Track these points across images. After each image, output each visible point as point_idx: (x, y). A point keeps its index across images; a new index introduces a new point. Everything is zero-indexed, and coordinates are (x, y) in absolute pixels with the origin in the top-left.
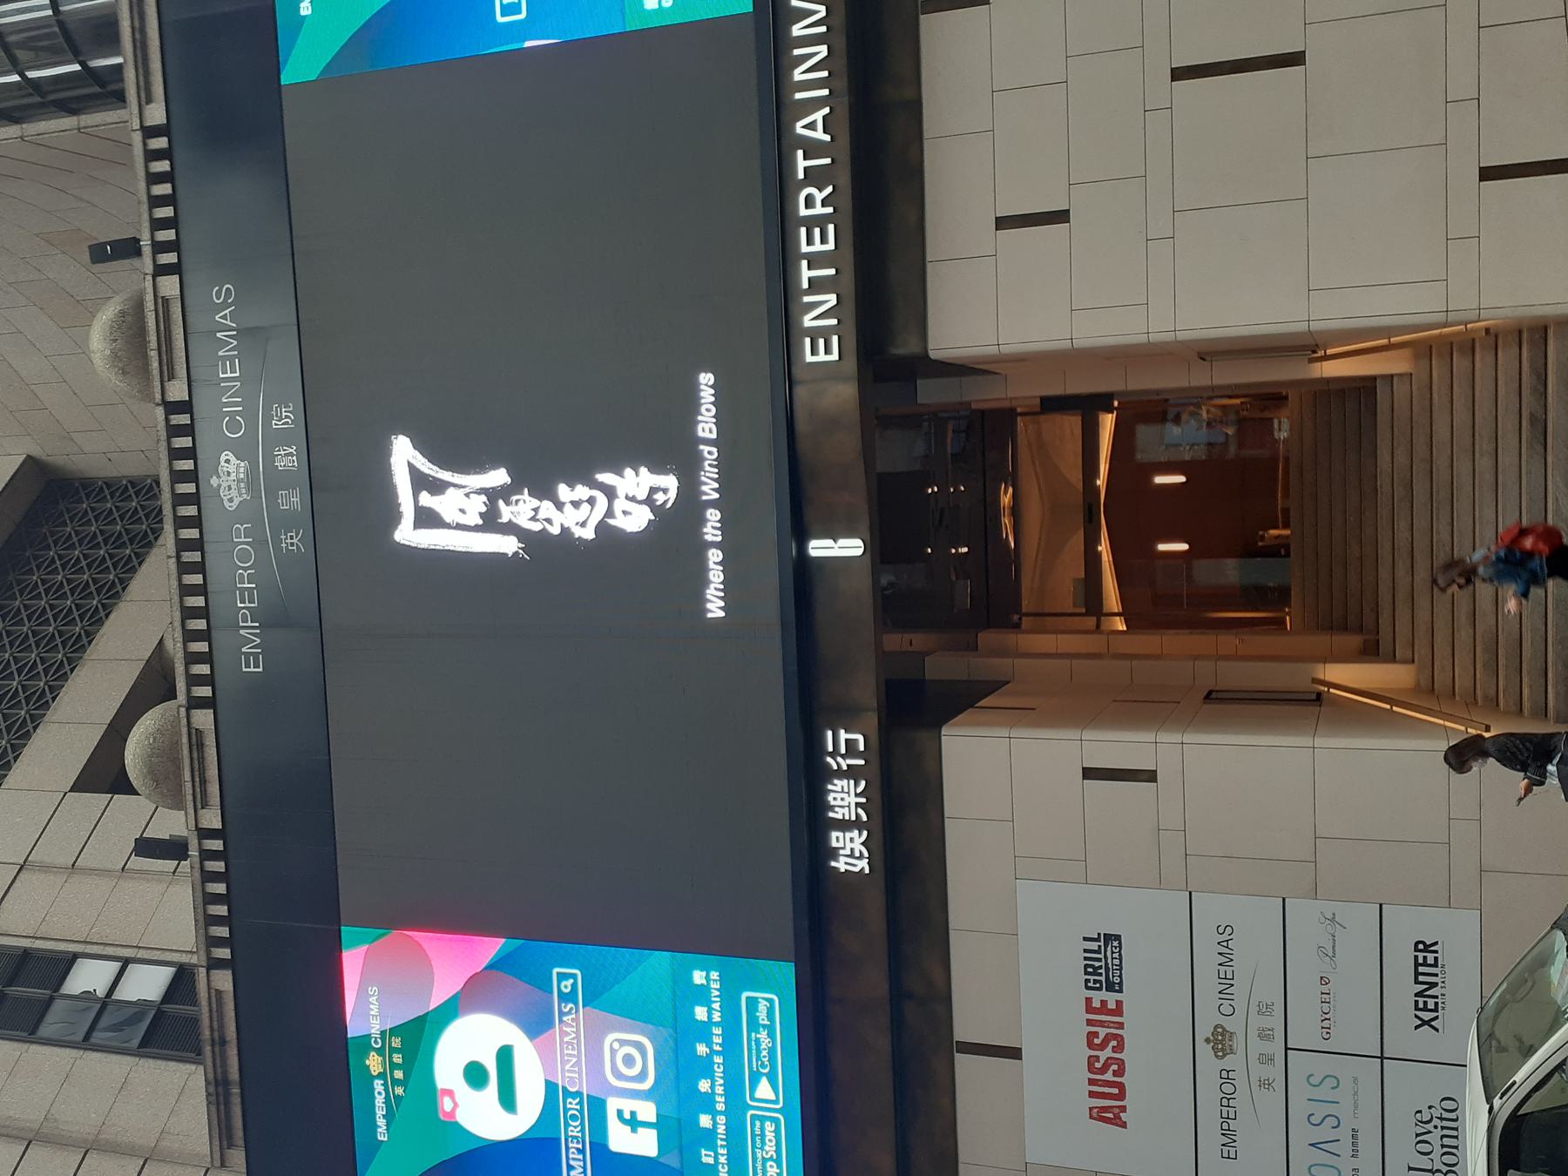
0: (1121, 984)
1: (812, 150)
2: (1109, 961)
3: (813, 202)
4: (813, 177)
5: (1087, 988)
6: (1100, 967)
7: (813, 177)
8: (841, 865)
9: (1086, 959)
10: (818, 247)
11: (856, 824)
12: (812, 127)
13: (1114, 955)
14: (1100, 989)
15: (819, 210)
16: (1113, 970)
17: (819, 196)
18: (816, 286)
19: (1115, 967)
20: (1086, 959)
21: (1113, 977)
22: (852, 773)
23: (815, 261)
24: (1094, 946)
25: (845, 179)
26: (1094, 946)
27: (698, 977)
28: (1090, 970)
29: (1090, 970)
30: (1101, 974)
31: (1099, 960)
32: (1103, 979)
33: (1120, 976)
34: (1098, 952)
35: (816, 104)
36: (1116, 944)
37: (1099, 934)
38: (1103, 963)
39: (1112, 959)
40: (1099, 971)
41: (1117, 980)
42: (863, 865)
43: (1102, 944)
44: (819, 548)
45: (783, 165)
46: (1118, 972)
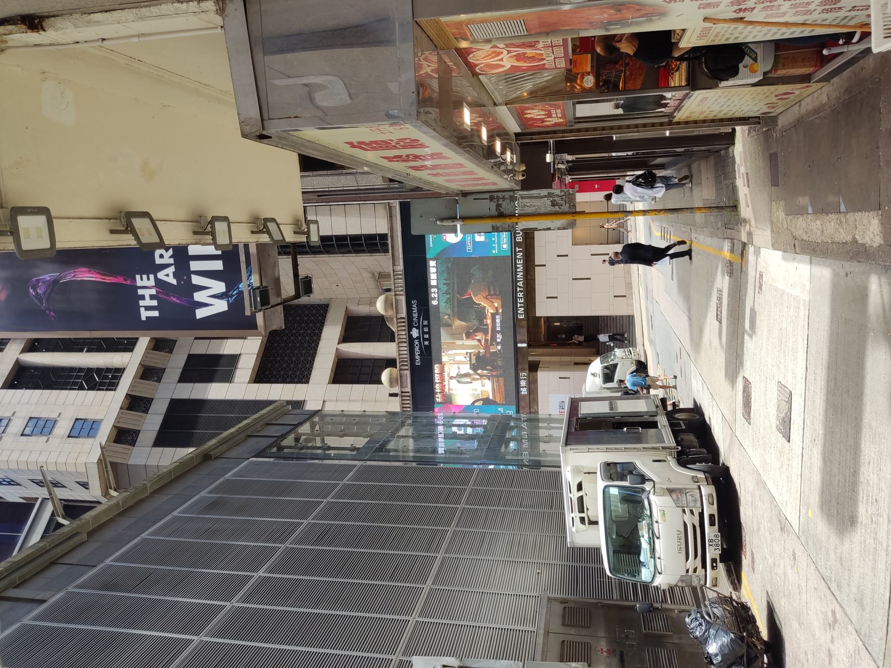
1: (520, 287)
3: (520, 295)
4: (520, 291)
7: (520, 291)
8: (522, 393)
10: (521, 301)
11: (525, 387)
12: (520, 284)
15: (521, 296)
17: (521, 294)
18: (520, 307)
22: (524, 379)
23: (520, 303)
25: (525, 292)
27: (499, 409)
35: (521, 281)
42: (526, 393)
44: (519, 345)
45: (516, 289)
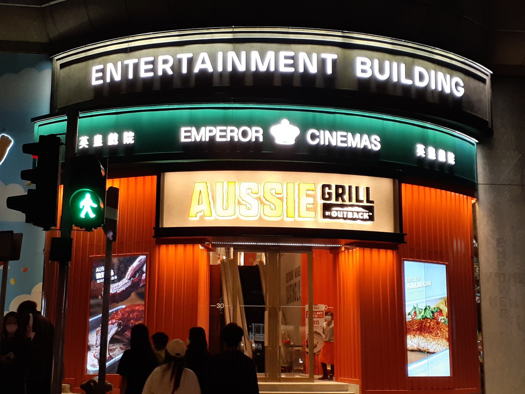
0: (330, 217)
2: (349, 209)
5: (324, 186)
6: (343, 200)
9: (350, 187)
13: (355, 214)
14: (323, 198)
16: (343, 211)
19: (345, 213)
20: (350, 187)
21: (337, 211)
24: (362, 196)
26: (362, 196)
28: (340, 191)
29: (340, 191)
30: (337, 200)
31: (350, 199)
32: (333, 201)
33: (337, 218)
34: (358, 200)
36: (366, 216)
37: (372, 202)
38: (347, 203)
39: (353, 212)
40: (340, 198)
41: (334, 214)
43: (365, 204)
46: (342, 217)
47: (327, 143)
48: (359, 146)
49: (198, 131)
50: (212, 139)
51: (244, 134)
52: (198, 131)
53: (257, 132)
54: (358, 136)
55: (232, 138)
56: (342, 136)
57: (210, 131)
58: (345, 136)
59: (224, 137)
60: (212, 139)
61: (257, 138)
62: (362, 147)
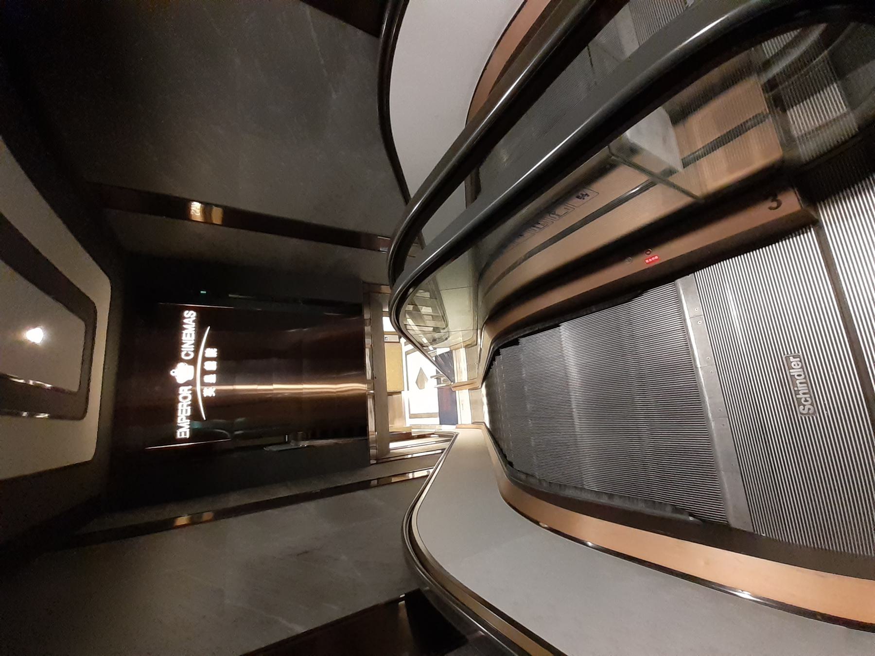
47: (193, 346)
48: (194, 326)
49: (181, 427)
50: (187, 418)
51: (185, 398)
52: (181, 427)
53: (183, 390)
54: (185, 326)
55: (188, 405)
56: (186, 336)
57: (182, 420)
58: (186, 334)
59: (187, 410)
60: (187, 418)
61: (189, 390)
62: (194, 324)
